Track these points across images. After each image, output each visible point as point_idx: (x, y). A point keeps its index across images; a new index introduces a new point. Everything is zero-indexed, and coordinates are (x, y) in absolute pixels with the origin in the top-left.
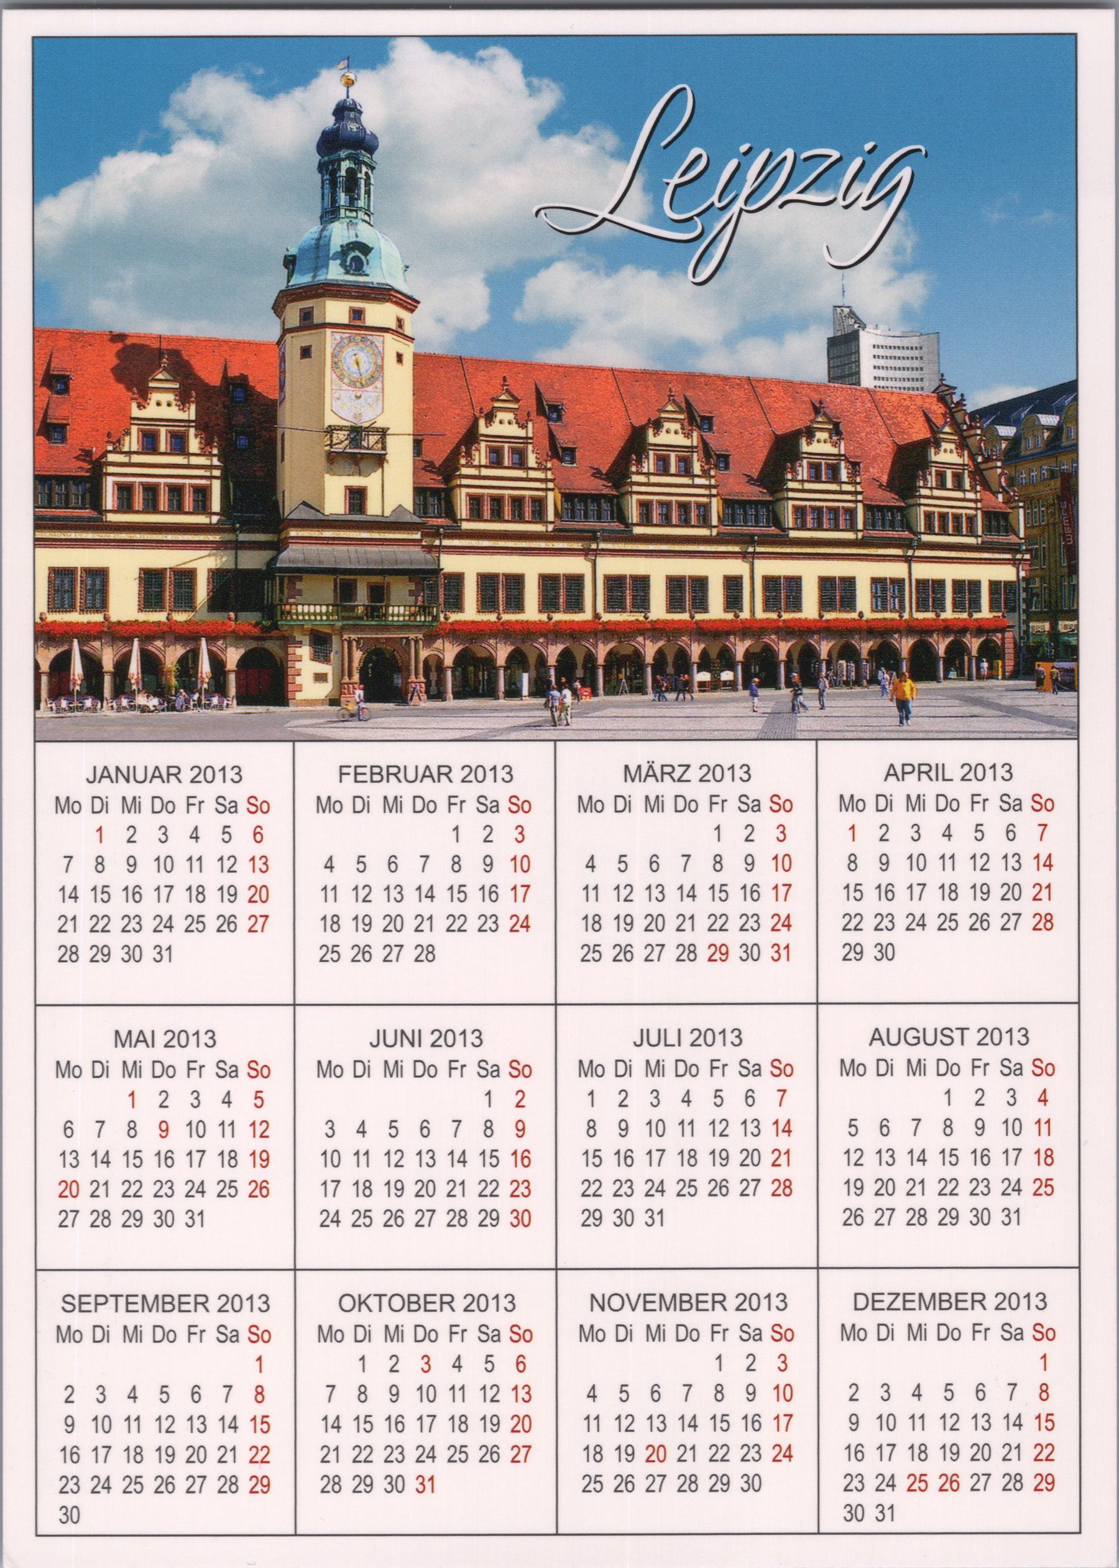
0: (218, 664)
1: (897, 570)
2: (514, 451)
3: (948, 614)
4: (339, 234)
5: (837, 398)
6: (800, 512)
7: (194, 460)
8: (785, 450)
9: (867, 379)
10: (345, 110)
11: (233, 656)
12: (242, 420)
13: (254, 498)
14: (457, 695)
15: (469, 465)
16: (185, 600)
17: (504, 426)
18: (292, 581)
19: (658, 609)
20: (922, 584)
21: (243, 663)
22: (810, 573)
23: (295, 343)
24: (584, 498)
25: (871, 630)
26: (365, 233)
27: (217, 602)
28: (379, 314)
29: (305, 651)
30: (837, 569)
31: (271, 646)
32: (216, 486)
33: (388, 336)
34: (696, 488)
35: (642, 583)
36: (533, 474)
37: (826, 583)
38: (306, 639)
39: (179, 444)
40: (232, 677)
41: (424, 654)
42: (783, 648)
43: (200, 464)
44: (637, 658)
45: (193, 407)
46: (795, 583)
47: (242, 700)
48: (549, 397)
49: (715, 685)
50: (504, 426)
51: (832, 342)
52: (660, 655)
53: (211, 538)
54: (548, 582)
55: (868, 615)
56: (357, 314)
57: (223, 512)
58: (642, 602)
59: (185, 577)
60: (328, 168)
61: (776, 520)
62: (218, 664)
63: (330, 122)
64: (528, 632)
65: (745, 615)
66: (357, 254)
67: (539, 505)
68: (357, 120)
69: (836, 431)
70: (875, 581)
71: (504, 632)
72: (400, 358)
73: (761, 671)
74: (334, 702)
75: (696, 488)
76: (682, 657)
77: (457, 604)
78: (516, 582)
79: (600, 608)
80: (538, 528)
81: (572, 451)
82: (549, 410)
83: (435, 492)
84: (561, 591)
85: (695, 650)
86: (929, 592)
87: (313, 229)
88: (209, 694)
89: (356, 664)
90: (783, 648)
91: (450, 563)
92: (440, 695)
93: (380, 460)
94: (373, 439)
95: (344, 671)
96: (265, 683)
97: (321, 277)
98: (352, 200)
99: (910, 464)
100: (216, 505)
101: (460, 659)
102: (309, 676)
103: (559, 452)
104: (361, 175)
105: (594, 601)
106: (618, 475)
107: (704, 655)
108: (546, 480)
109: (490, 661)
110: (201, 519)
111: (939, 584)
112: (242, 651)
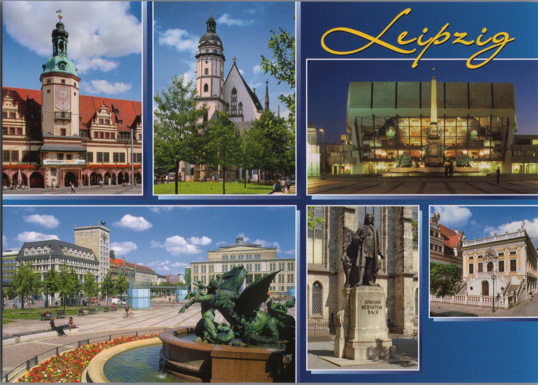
0: (24, 177)
2: (106, 120)
4: (58, 59)
7: (18, 121)
10: (59, 25)
11: (29, 174)
12: (31, 110)
13: (35, 131)
14: (91, 184)
15: (94, 124)
18: (46, 153)
21: (32, 176)
23: (46, 89)
24: (125, 133)
26: (65, 59)
27: (25, 159)
28: (70, 81)
29: (49, 173)
31: (39, 171)
32: (24, 128)
33: (72, 88)
36: (111, 126)
38: (50, 170)
39: (13, 116)
40: (29, 180)
41: (82, 173)
43: (19, 122)
45: (17, 106)
47: (31, 187)
53: (22, 142)
54: (116, 155)
59: (16, 153)
60: (55, 41)
62: (24, 177)
63: (55, 28)
64: (111, 167)
66: (63, 64)
67: (113, 134)
68: (63, 28)
71: (105, 167)
72: (75, 94)
77: (91, 160)
78: (107, 155)
79: (129, 161)
80: (113, 140)
83: (85, 130)
84: (119, 157)
87: (51, 58)
88: (22, 184)
89: (64, 176)
91: (89, 149)
93: (69, 121)
95: (60, 178)
97: (53, 70)
98: (62, 51)
100: (24, 132)
101: (92, 175)
104: (64, 43)
105: (128, 160)
108: (115, 128)
109: (100, 175)
112: (32, 173)
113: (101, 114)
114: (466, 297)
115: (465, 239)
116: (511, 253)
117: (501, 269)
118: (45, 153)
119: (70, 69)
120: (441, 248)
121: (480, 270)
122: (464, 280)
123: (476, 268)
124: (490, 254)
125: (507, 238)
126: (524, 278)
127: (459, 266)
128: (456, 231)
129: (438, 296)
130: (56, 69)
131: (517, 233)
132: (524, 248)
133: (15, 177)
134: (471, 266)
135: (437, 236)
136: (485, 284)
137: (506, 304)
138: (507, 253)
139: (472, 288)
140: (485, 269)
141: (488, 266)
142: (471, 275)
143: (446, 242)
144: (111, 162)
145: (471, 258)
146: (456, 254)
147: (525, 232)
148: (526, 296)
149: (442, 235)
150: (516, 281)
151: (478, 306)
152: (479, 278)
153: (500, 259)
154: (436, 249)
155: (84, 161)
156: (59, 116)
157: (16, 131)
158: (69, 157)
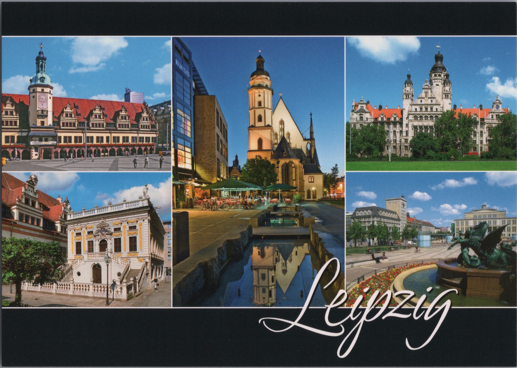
0: (18, 152)
1: (136, 135)
3: (144, 143)
4: (40, 75)
5: (126, 106)
6: (119, 125)
8: (117, 114)
9: (131, 101)
11: (21, 151)
13: (25, 123)
16: (13, 141)
17: (68, 110)
19: (95, 142)
20: (140, 138)
22: (121, 136)
25: (131, 146)
27: (18, 142)
28: (47, 90)
29: (33, 150)
30: (126, 135)
31: (28, 149)
34: (101, 121)
35: (92, 137)
37: (124, 137)
39: (12, 114)
41: (54, 150)
42: (116, 149)
44: (91, 150)
46: (118, 138)
48: (76, 105)
49: (104, 156)
50: (68, 110)
51: (125, 95)
52: (95, 150)
55: (131, 143)
56: (43, 90)
57: (19, 126)
58: (92, 141)
59: (13, 137)
61: (115, 126)
64: (72, 146)
65: (110, 143)
66: (43, 79)
67: (74, 124)
69: (126, 110)
70: (132, 137)
71: (68, 146)
73: (112, 153)
74: (38, 159)
75: (101, 121)
76: (99, 150)
77: (60, 141)
78: (70, 138)
81: (80, 115)
82: (76, 107)
85: (101, 149)
86: (141, 139)
87: (35, 75)
90: (116, 149)
91: (59, 134)
92: (57, 158)
93: (47, 116)
94: (45, 112)
96: (27, 156)
99: (138, 116)
100: (18, 124)
101: (61, 151)
102: (34, 155)
103: (77, 114)
106: (88, 119)
107: (103, 150)
109: (66, 152)
110: (15, 127)
111: (143, 138)
113: (67, 110)
118: (31, 138)
119: (48, 81)
130: (39, 82)
133: (13, 153)
144: (73, 143)
155: (55, 142)
156: (40, 113)
157: (13, 123)
158: (46, 140)
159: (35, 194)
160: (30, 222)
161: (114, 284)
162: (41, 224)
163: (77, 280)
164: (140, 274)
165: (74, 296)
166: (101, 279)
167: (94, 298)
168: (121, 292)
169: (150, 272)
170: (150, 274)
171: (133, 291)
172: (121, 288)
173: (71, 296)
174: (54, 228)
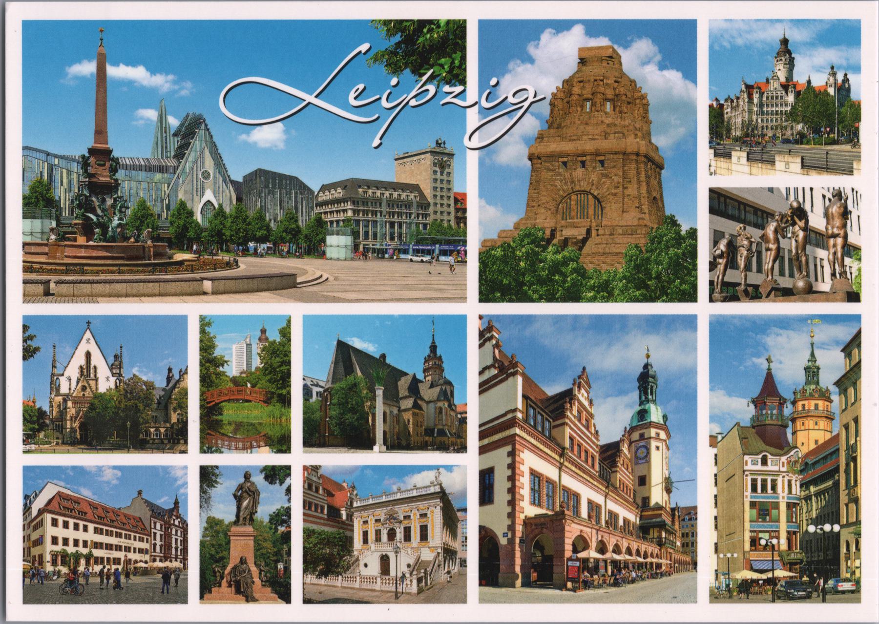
114: (358, 578)
115: (357, 495)
116: (421, 515)
117: (407, 537)
120: (322, 508)
121: (378, 539)
122: (356, 553)
123: (372, 536)
124: (392, 517)
125: (415, 493)
126: (439, 550)
127: (348, 533)
128: (345, 485)
129: (319, 576)
131: (429, 487)
132: (438, 508)
134: (365, 534)
135: (317, 491)
136: (385, 561)
137: (414, 588)
138: (415, 516)
139: (366, 565)
140: (384, 537)
141: (388, 534)
142: (365, 546)
143: (330, 499)
145: (366, 522)
146: (344, 517)
147: (441, 485)
148: (441, 576)
149: (324, 489)
150: (427, 555)
151: (374, 590)
152: (376, 551)
153: (406, 523)
154: (316, 511)
159: (319, 478)
160: (313, 509)
161: (404, 576)
162: (326, 512)
163: (364, 572)
164: (431, 566)
165: (361, 589)
166: (389, 571)
167: (382, 591)
168: (411, 585)
169: (442, 563)
170: (442, 566)
171: (423, 584)
172: (411, 581)
173: (357, 589)
174: (340, 516)
